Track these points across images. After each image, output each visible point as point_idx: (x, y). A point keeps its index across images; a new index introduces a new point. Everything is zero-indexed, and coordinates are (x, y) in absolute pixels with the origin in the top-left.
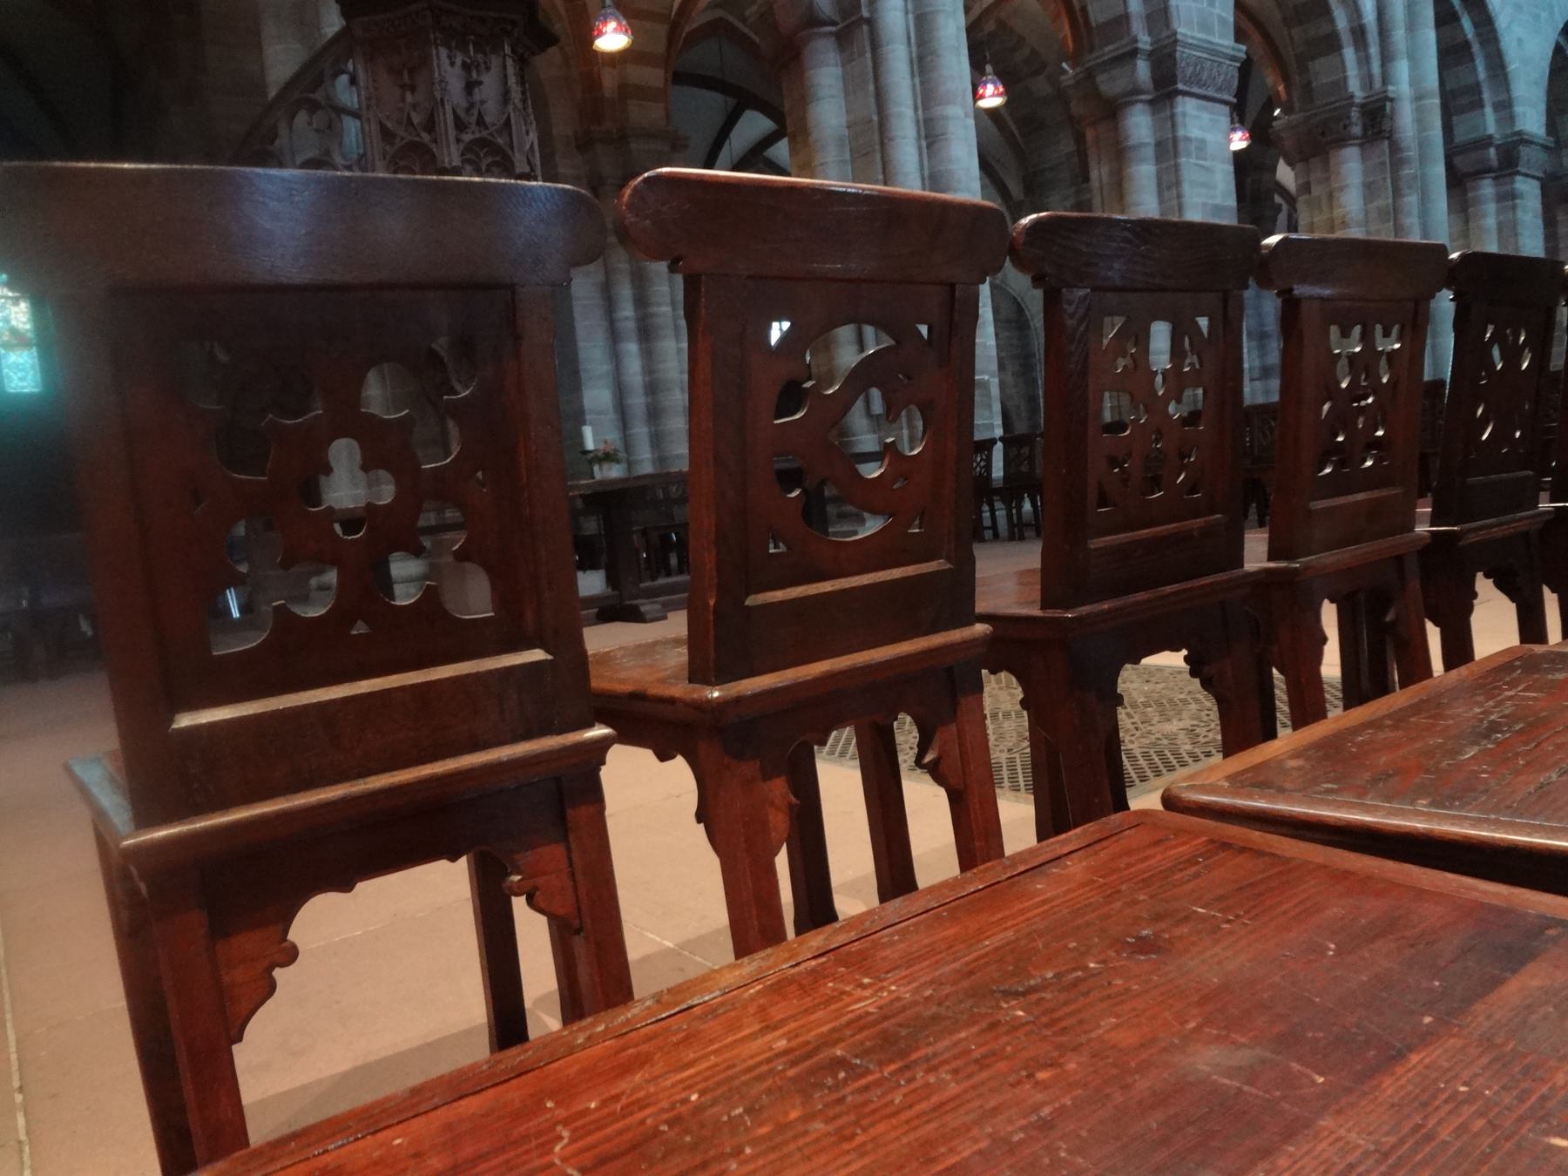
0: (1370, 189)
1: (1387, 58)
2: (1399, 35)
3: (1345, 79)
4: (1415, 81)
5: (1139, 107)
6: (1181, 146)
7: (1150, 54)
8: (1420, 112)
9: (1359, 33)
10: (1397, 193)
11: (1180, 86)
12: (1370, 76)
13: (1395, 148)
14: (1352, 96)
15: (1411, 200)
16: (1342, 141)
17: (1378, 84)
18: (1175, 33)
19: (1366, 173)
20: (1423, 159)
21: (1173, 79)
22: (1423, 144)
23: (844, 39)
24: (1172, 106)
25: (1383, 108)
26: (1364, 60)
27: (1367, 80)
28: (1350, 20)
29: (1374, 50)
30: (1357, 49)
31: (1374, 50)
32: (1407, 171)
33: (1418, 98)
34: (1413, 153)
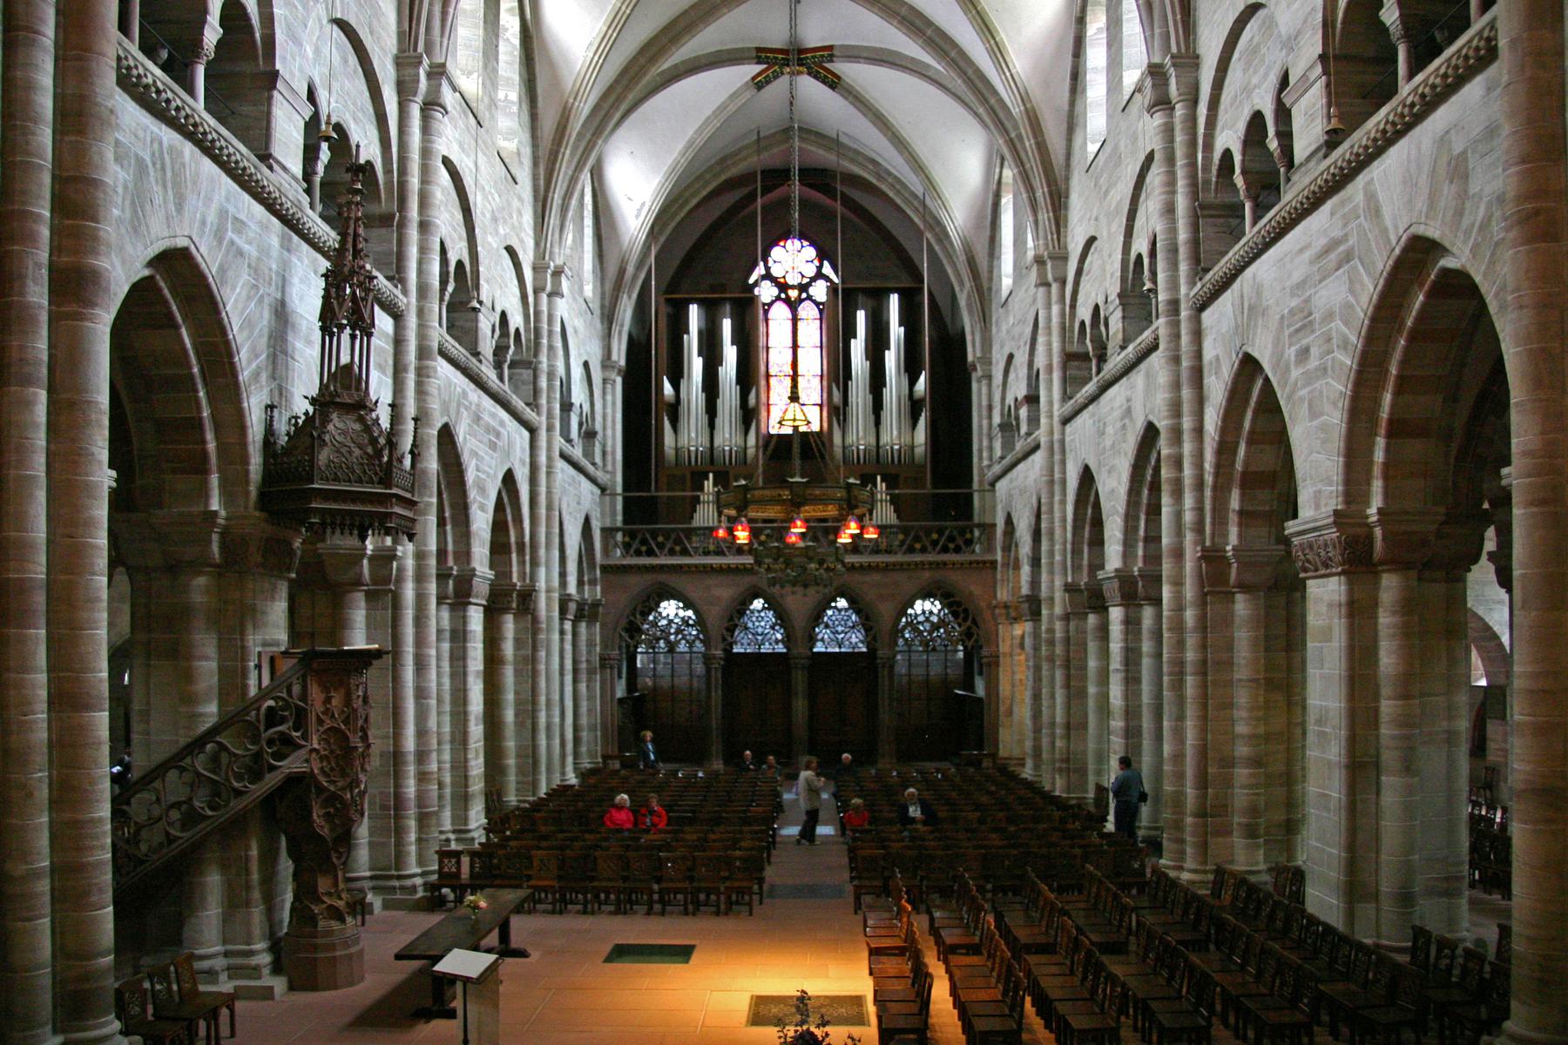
0: (518, 642)
1: (535, 563)
2: (542, 552)
3: (511, 572)
4: (548, 581)
5: (445, 607)
6: (469, 636)
7: (457, 576)
8: (549, 599)
9: (521, 546)
10: (535, 648)
11: (472, 600)
12: (525, 573)
13: (535, 620)
14: (515, 585)
15: (542, 654)
16: (506, 610)
17: (528, 581)
18: (474, 569)
19: (517, 631)
20: (549, 630)
21: (469, 595)
22: (549, 618)
23: (371, 596)
24: (465, 611)
25: (530, 595)
26: (522, 563)
27: (522, 575)
28: (517, 538)
29: (528, 558)
30: (518, 555)
31: (528, 558)
32: (542, 636)
33: (548, 591)
34: (544, 626)
